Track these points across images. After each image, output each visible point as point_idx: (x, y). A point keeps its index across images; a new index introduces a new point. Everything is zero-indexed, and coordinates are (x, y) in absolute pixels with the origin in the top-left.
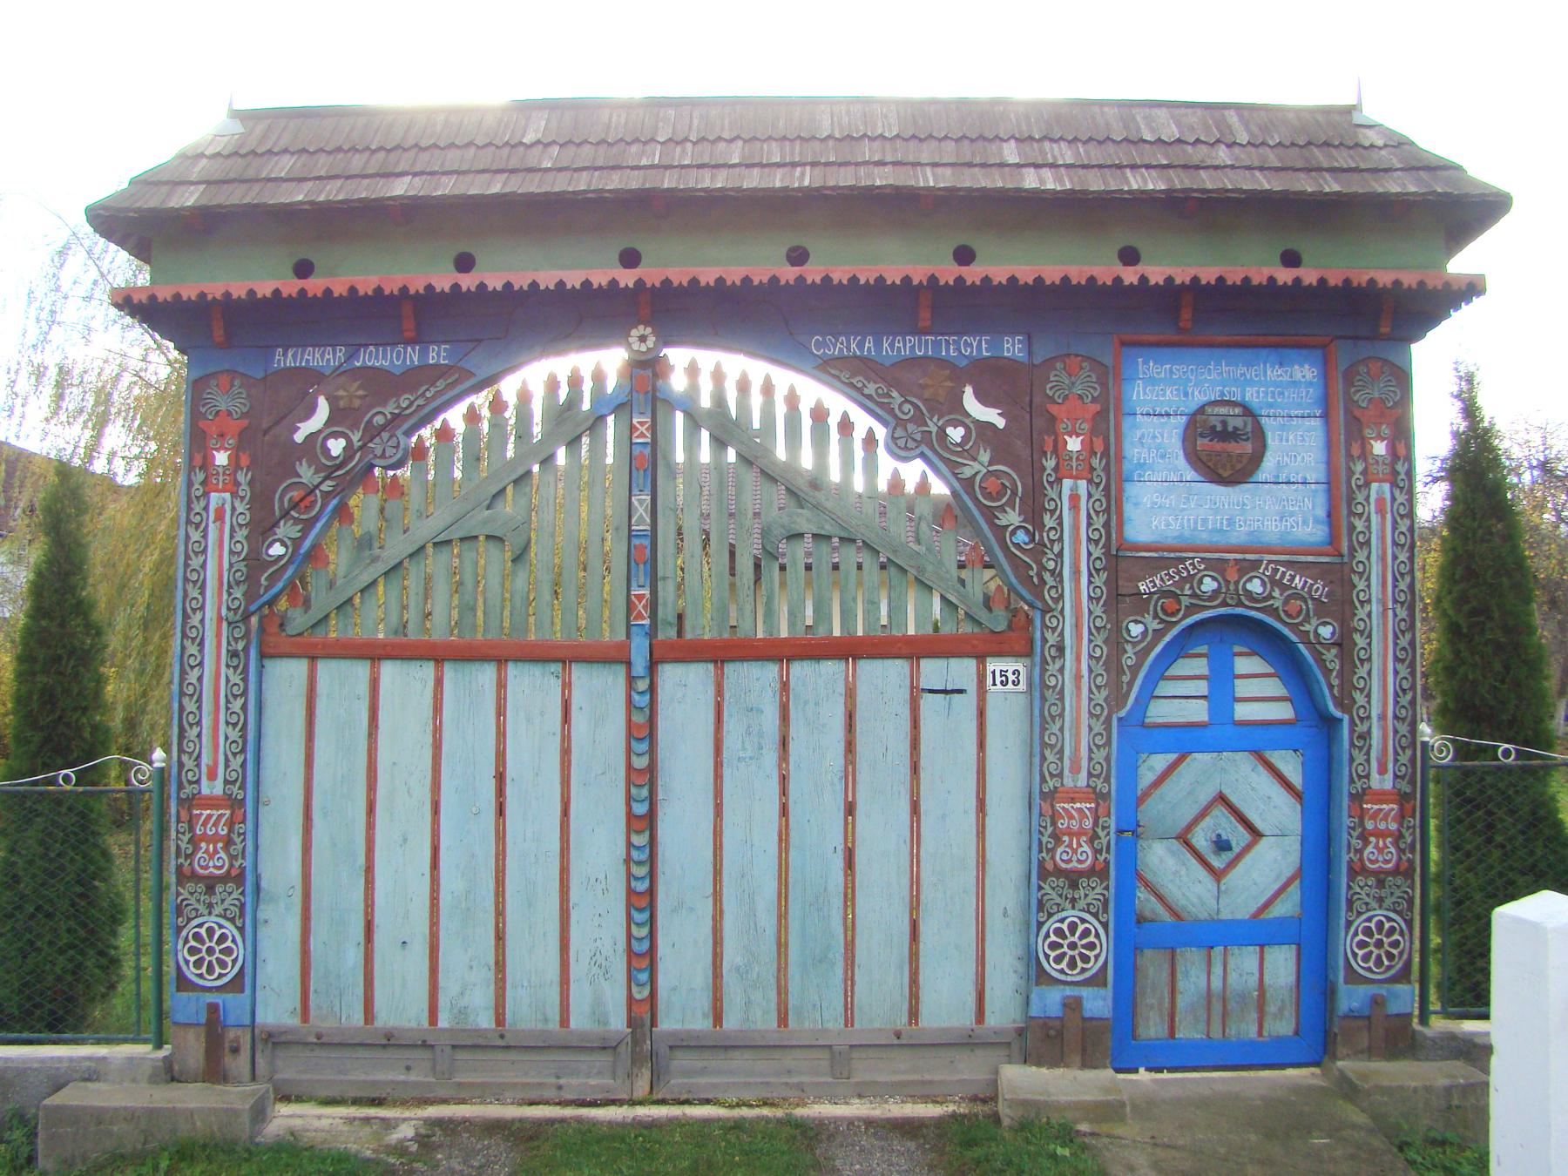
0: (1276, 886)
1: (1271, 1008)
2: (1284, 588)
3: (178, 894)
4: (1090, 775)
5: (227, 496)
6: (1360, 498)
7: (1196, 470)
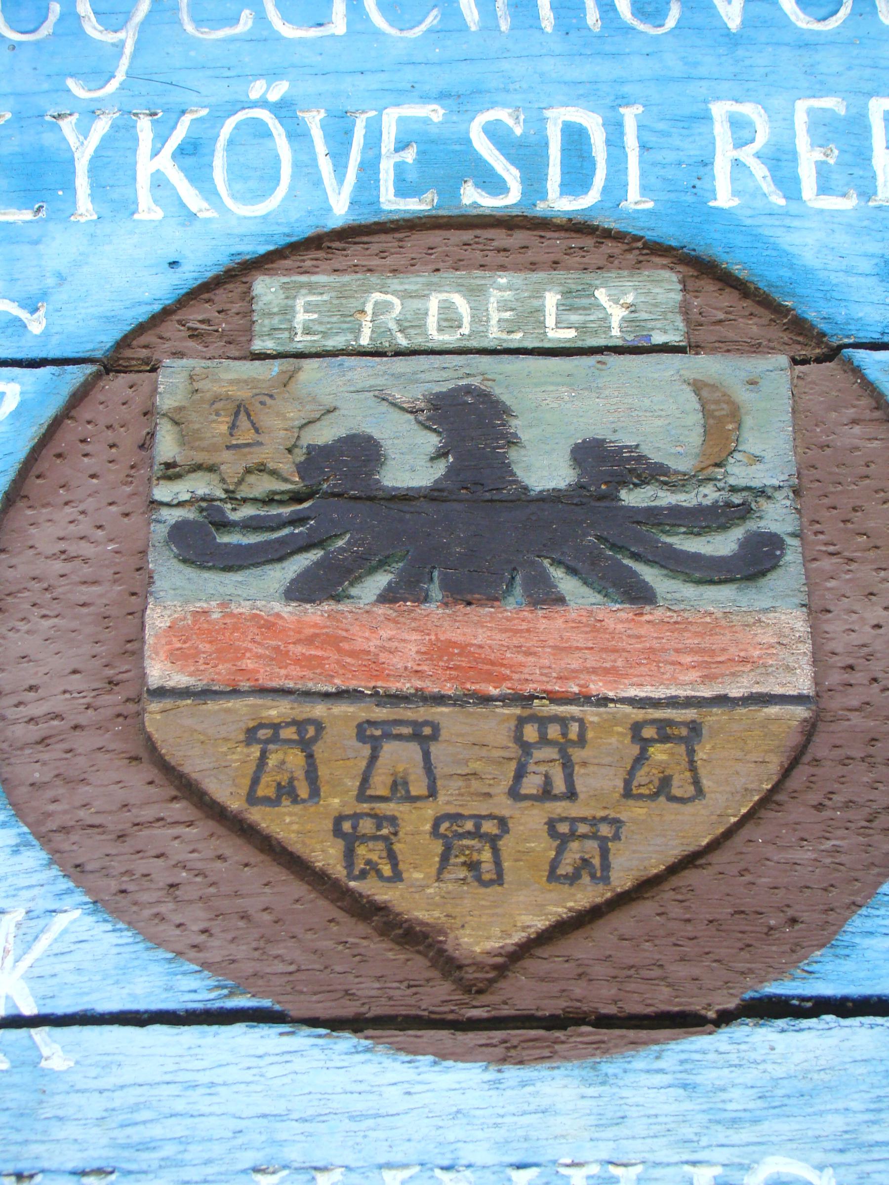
7: (115, 900)
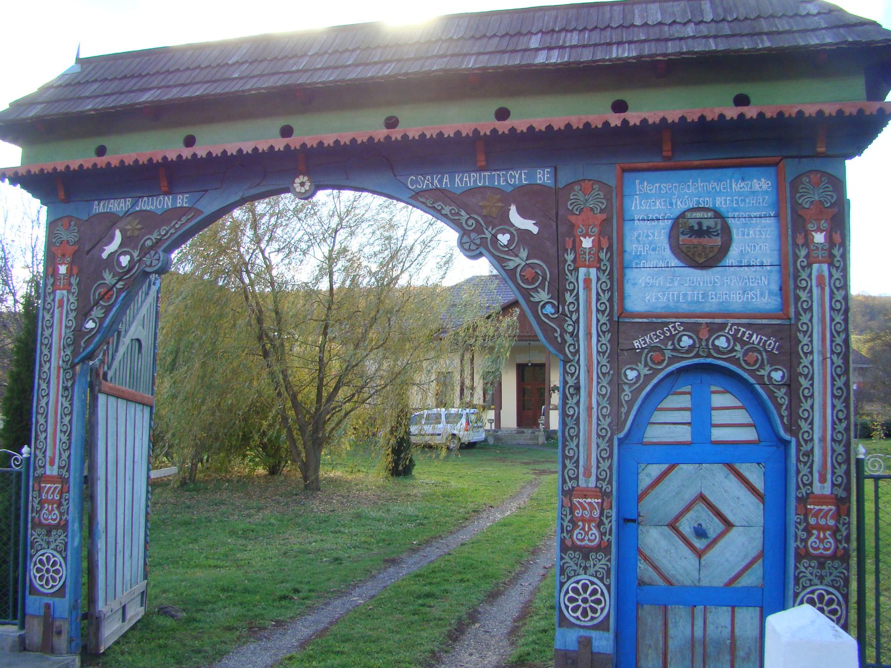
0: (744, 564)
1: (741, 653)
2: (744, 343)
3: (32, 535)
4: (598, 479)
5: (65, 292)
6: (804, 275)
7: (679, 259)
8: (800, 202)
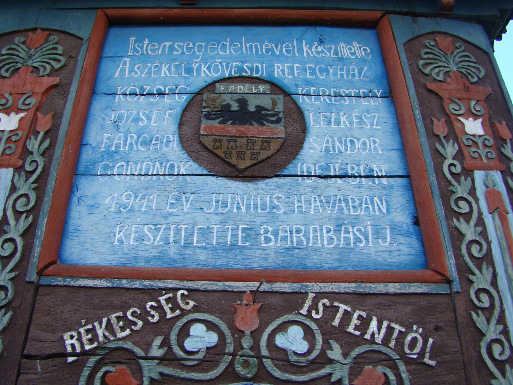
6: (461, 190)
8: (427, 71)
